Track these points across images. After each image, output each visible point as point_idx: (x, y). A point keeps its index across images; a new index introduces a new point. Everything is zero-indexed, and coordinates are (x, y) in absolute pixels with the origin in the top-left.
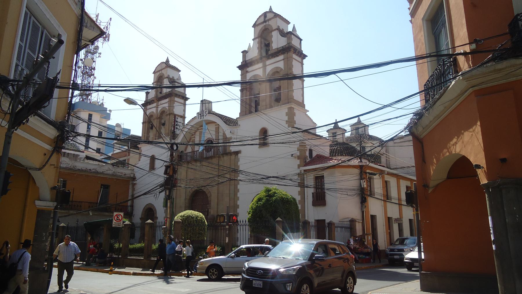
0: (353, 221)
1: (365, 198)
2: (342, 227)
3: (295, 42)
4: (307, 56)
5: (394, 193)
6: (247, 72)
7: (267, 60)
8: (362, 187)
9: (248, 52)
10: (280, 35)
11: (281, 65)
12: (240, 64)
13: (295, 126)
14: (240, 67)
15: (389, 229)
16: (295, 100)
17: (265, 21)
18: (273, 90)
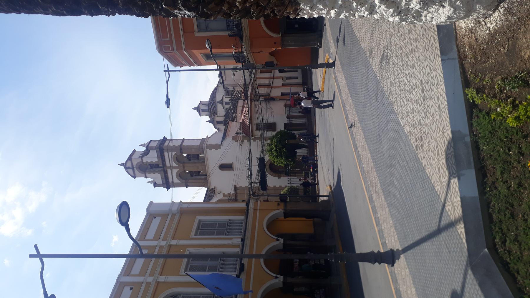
0: (286, 106)
1: (271, 98)
2: (290, 112)
3: (154, 145)
4: (164, 136)
5: (266, 81)
6: (173, 182)
7: (166, 166)
8: (264, 99)
9: (155, 182)
10: (147, 156)
11: (171, 155)
12: (166, 188)
13: (220, 143)
14: (168, 189)
15: (289, 85)
16: (200, 145)
17: (133, 168)
18: (190, 161)
